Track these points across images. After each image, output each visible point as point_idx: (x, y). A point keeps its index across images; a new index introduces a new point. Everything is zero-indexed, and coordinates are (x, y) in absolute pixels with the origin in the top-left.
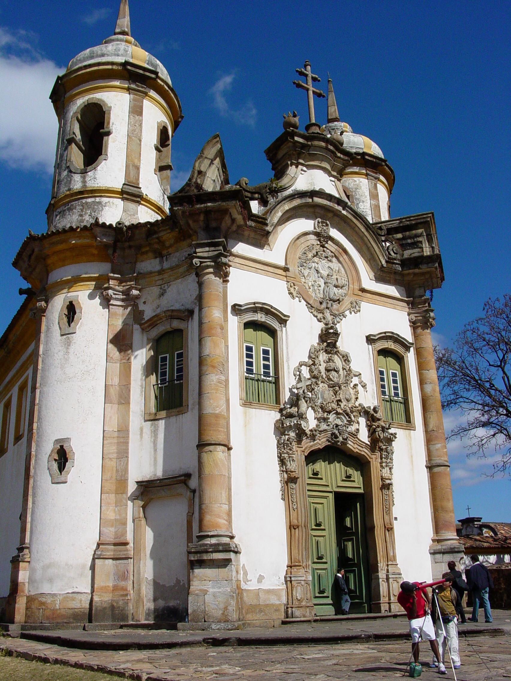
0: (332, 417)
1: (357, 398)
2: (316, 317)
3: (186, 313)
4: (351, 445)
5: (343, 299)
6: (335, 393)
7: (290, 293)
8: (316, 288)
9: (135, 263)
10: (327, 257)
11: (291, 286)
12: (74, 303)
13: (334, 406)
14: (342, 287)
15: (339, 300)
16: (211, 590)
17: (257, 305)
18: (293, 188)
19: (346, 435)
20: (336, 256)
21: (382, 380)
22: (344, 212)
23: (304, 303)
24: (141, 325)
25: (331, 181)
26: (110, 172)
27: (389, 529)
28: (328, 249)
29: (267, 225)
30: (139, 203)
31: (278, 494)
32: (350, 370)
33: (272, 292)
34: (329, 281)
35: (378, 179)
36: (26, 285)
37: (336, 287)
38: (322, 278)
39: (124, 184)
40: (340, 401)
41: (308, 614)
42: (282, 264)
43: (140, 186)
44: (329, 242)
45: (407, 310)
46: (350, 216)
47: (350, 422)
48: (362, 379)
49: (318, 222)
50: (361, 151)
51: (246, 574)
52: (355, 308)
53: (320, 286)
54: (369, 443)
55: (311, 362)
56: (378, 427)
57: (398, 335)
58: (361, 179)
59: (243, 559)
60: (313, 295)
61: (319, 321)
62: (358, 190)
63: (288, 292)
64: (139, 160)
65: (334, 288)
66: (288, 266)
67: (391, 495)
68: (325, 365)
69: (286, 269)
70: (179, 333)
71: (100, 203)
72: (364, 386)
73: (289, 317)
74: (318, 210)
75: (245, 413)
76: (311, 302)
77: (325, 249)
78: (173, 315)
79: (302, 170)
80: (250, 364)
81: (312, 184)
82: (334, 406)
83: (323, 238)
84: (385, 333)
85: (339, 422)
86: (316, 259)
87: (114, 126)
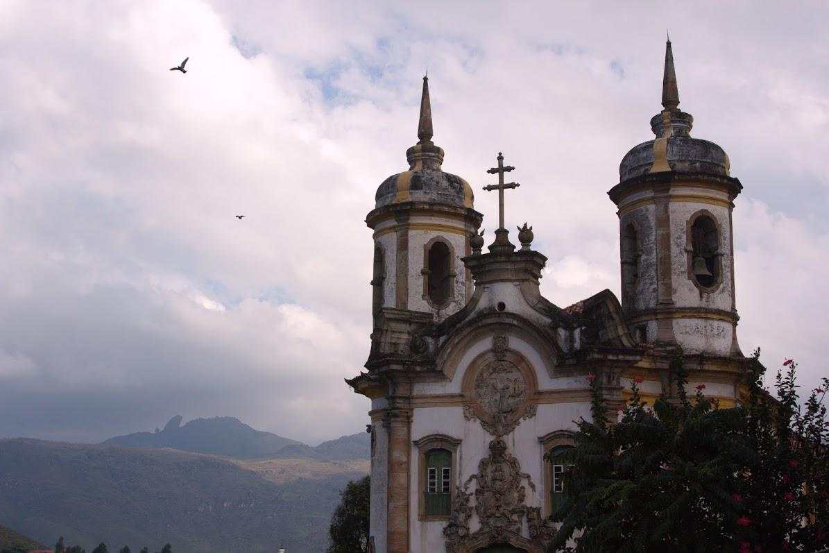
0: (492, 521)
2: (489, 431)
4: (513, 541)
5: (518, 408)
6: (497, 500)
7: (465, 416)
8: (492, 404)
10: (506, 370)
14: (519, 395)
18: (477, 309)
19: (504, 534)
22: (515, 322)
23: (478, 421)
29: (436, 365)
32: (517, 474)
37: (513, 396)
44: (508, 354)
48: (532, 480)
49: (495, 339)
54: (529, 538)
55: (480, 475)
56: (531, 526)
57: (570, 432)
58: (648, 206)
62: (644, 222)
68: (492, 474)
69: (461, 396)
72: (533, 486)
73: (458, 440)
74: (492, 327)
76: (486, 418)
77: (502, 362)
79: (484, 288)
80: (433, 484)
82: (493, 511)
84: (554, 432)
85: (499, 524)
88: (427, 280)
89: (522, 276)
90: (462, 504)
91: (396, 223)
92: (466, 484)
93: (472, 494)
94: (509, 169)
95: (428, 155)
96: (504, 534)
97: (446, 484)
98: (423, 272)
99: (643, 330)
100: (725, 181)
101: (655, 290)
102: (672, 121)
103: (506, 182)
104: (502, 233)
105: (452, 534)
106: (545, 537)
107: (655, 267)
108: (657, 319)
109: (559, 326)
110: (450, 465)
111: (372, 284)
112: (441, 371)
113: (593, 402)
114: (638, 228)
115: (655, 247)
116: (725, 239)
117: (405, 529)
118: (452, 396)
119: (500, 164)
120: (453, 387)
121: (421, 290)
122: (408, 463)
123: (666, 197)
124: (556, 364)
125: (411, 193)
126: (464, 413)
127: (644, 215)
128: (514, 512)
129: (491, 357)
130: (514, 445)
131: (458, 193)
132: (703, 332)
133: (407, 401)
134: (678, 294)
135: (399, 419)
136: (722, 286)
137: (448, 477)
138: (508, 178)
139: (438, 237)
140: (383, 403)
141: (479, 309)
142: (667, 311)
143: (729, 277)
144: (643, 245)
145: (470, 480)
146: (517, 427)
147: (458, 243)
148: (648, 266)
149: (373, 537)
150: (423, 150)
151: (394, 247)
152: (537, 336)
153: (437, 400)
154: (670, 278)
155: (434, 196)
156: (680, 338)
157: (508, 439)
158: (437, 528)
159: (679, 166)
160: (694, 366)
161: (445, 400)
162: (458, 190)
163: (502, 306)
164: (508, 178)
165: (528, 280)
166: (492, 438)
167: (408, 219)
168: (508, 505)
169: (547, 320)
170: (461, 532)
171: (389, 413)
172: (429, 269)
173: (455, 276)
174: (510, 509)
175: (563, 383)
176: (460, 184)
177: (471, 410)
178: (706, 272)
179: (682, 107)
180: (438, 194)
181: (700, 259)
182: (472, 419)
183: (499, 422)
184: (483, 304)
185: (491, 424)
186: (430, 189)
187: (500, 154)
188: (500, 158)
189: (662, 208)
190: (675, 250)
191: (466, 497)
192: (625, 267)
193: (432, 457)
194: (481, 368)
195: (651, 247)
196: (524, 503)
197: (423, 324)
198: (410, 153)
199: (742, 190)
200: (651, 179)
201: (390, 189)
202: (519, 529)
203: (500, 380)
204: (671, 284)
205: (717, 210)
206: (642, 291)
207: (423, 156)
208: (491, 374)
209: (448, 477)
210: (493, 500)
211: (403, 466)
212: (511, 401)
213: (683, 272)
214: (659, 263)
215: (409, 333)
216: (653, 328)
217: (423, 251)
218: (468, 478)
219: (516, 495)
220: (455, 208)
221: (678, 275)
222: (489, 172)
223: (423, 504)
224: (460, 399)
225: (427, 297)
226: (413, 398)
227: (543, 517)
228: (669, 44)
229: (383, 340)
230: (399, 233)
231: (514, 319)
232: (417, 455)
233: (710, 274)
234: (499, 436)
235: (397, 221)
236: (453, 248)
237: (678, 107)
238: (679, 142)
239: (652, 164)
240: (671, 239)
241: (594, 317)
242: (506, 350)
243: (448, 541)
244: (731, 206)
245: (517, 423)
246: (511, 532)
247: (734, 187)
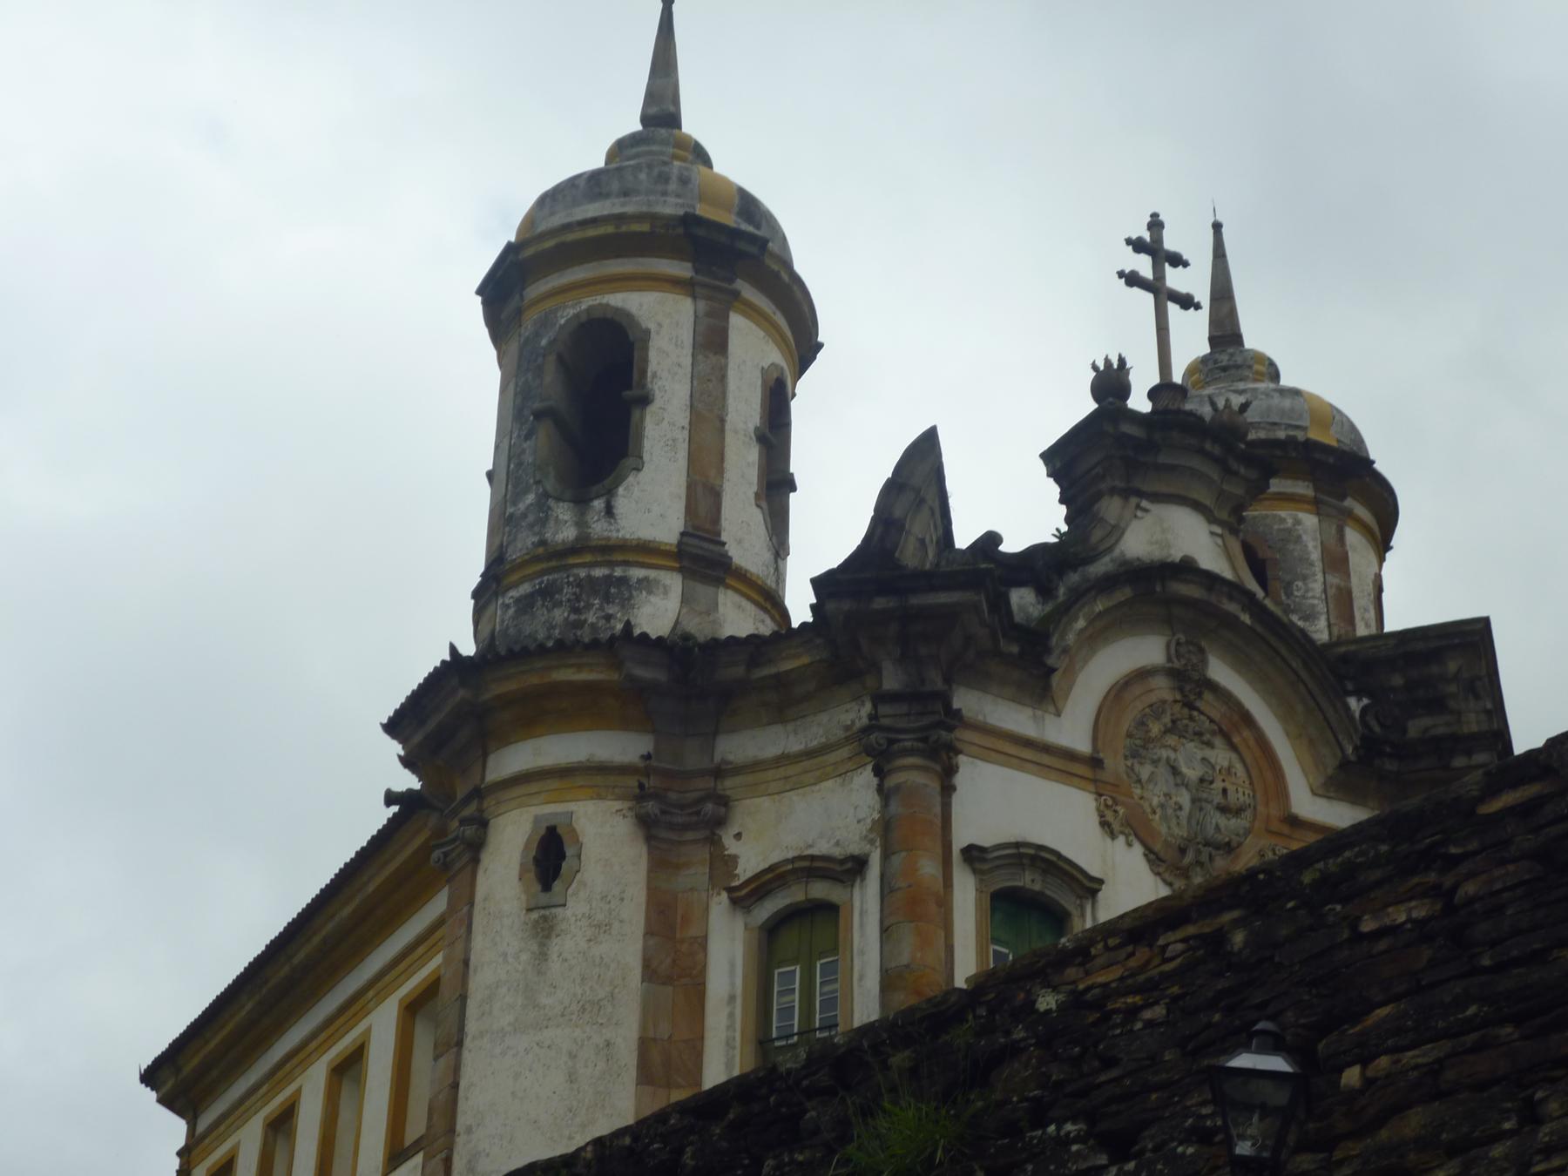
3: (849, 865)
5: (1240, 845)
7: (1104, 824)
8: (1170, 811)
9: (715, 734)
10: (1199, 734)
11: (1107, 806)
12: (560, 831)
14: (1238, 812)
15: (1228, 844)
17: (1022, 850)
18: (1117, 552)
20: (1221, 730)
22: (1246, 618)
23: (1138, 849)
24: (730, 890)
25: (1212, 533)
26: (650, 505)
28: (1202, 713)
30: (719, 582)
33: (1062, 819)
34: (1205, 795)
35: (1349, 515)
36: (408, 781)
37: (1223, 809)
38: (1187, 786)
39: (683, 534)
42: (1083, 746)
43: (724, 538)
44: (1208, 696)
46: (1259, 629)
49: (1178, 644)
50: (1300, 436)
53: (1180, 808)
58: (1301, 515)
60: (1164, 829)
62: (1291, 547)
64: (721, 471)
65: (1218, 814)
66: (1101, 755)
69: (1095, 762)
70: (828, 911)
71: (623, 581)
73: (1101, 882)
76: (1158, 847)
78: (811, 867)
79: (1138, 507)
83: (1189, 682)
86: (1171, 740)
115: (1322, 607)
118: (1070, 755)
124: (1353, 758)
126: (1102, 816)
127: (1289, 531)
129: (1162, 688)
141: (1123, 554)
144: (1289, 594)
151: (687, 336)
152: (1304, 674)
153: (1028, 754)
161: (1046, 759)
167: (731, 281)
171: (891, 742)
188: (1156, 224)
189: (1333, 530)
195: (1313, 606)
201: (673, 186)
208: (1167, 731)
212: (1221, 820)
217: (759, 383)
222: (1129, 242)
228: (1217, 227)
230: (702, 304)
241: (1397, 680)
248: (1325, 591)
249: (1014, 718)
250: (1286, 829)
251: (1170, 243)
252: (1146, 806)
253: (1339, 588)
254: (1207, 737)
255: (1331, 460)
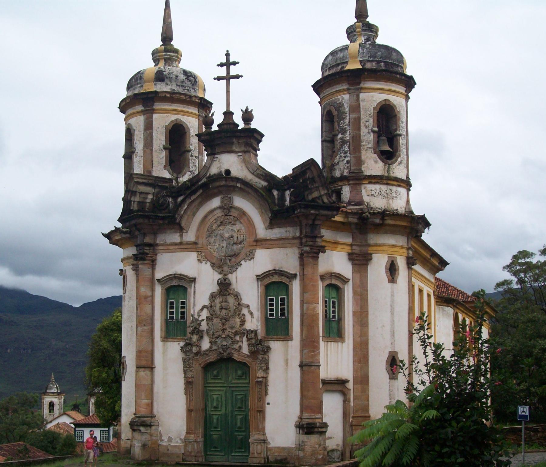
0: (219, 341)
1: (242, 324)
4: (236, 356)
6: (223, 324)
7: (198, 260)
10: (230, 223)
13: (221, 332)
14: (241, 242)
16: (136, 445)
19: (228, 351)
21: (272, 305)
22: (239, 185)
23: (209, 263)
27: (261, 412)
29: (176, 219)
31: (183, 391)
37: (236, 244)
40: (226, 329)
41: (194, 460)
44: (233, 210)
45: (298, 245)
46: (243, 187)
47: (235, 342)
48: (251, 309)
49: (222, 198)
51: (161, 436)
52: (250, 256)
53: (223, 247)
54: (249, 354)
55: (210, 305)
57: (281, 271)
58: (344, 96)
59: (160, 429)
61: (220, 273)
63: (197, 259)
67: (263, 388)
69: (195, 243)
73: (192, 278)
75: (164, 345)
76: (214, 261)
77: (228, 217)
79: (214, 158)
80: (172, 313)
81: (220, 168)
84: (269, 271)
85: (224, 343)
86: (222, 227)
87: (136, 145)
88: (168, 153)
89: (243, 149)
90: (195, 328)
91: (143, 108)
92: (198, 313)
93: (203, 320)
94: (235, 63)
95: (169, 55)
96: (228, 351)
97: (183, 313)
98: (165, 148)
99: (339, 193)
100: (403, 77)
101: (348, 162)
102: (364, 30)
103: (232, 73)
104: (228, 114)
105: (188, 351)
106: (261, 353)
107: (348, 144)
108: (349, 185)
109: (273, 188)
110: (186, 297)
111: (123, 157)
112: (179, 224)
113: (299, 248)
114: (335, 113)
116: (402, 123)
117: (150, 349)
118: (188, 244)
119: (228, 59)
120: (190, 236)
121: (163, 161)
122: (153, 296)
123: (357, 89)
125: (155, 85)
127: (340, 103)
128: (236, 334)
129: (219, 213)
130: (237, 282)
131: (193, 85)
132: (385, 195)
133: (152, 248)
134: (366, 165)
135: (146, 262)
136: (399, 159)
137: (184, 307)
138: (234, 70)
139: (176, 120)
140: (132, 251)
141: (210, 175)
142: (357, 178)
143: (405, 153)
145: (202, 310)
146: (239, 267)
147: (193, 124)
148: (343, 142)
149: (125, 357)
150: (166, 50)
151: (142, 128)
154: (360, 153)
155: (175, 87)
156: (366, 199)
157: (232, 277)
158: (175, 348)
159: (368, 66)
160: (378, 221)
162: (193, 82)
163: (228, 172)
164: (234, 70)
165: (248, 152)
166: (220, 276)
167: (153, 105)
168: (232, 328)
169: (265, 184)
170: (195, 349)
172: (170, 145)
173: (190, 151)
174: (233, 331)
175: (277, 233)
176: (194, 78)
177: (203, 254)
178: (387, 148)
179: (370, 20)
180: (177, 85)
181: (384, 138)
182: (204, 262)
183: (226, 264)
184: (214, 170)
185: (218, 265)
186: (170, 81)
187: (227, 51)
188: (228, 55)
190: (364, 131)
191: (199, 322)
192: (325, 144)
193: (171, 293)
194: (211, 221)
196: (244, 327)
197: (165, 188)
198: (154, 53)
199: (415, 86)
200: (346, 75)
201: (139, 81)
202: (240, 347)
203: (226, 231)
204: (360, 157)
205: (397, 101)
206: (339, 162)
207: (165, 55)
208: (219, 226)
209: (184, 307)
210: (220, 325)
211: (148, 299)
212: (235, 247)
213: (370, 148)
214: (351, 140)
215: (153, 194)
216: (346, 192)
218: (201, 308)
219: (238, 320)
220: (191, 97)
221: (366, 150)
222: (218, 65)
223: (164, 329)
224: (195, 246)
225: (169, 167)
226: (157, 245)
227: (259, 338)
229: (132, 199)
231: (237, 182)
232: (160, 290)
233: (391, 150)
234: (226, 275)
235: (143, 106)
236: (188, 128)
237: (367, 20)
238: (368, 46)
239: (347, 63)
240: (361, 122)
241: (301, 181)
242: (231, 207)
243: (184, 357)
244: (407, 98)
245: (239, 264)
246: (234, 349)
247: (409, 83)
248: (349, 122)
249: (175, 238)
250: (255, 244)
251: (231, 60)
252: (212, 250)
253: (355, 119)
254: (233, 222)
255: (349, 74)
